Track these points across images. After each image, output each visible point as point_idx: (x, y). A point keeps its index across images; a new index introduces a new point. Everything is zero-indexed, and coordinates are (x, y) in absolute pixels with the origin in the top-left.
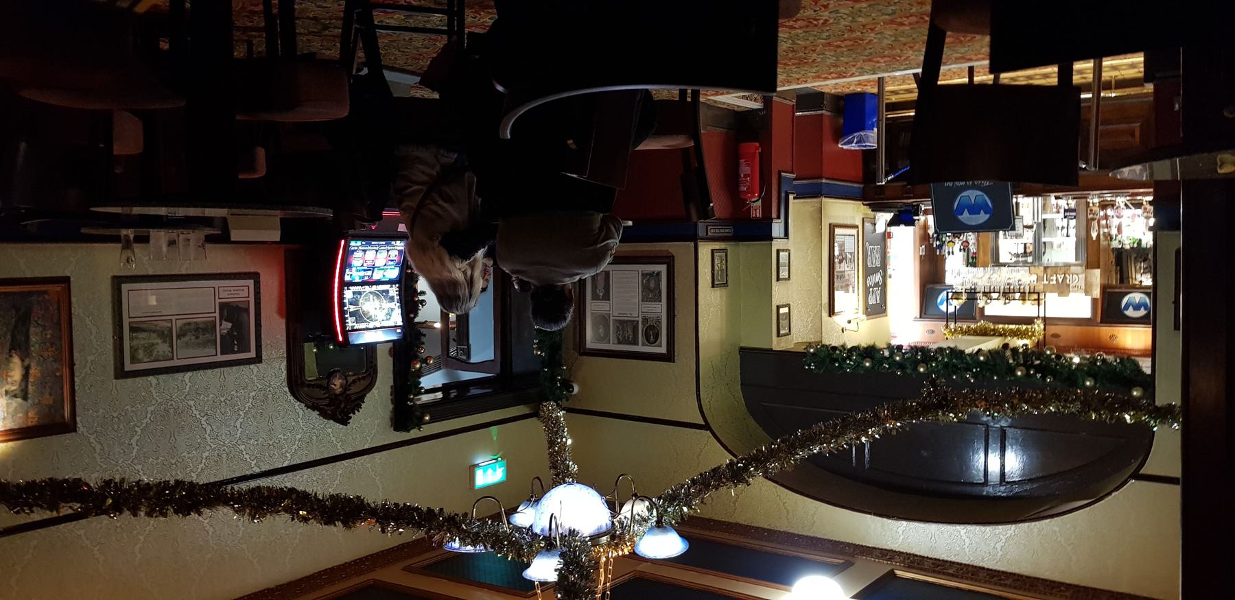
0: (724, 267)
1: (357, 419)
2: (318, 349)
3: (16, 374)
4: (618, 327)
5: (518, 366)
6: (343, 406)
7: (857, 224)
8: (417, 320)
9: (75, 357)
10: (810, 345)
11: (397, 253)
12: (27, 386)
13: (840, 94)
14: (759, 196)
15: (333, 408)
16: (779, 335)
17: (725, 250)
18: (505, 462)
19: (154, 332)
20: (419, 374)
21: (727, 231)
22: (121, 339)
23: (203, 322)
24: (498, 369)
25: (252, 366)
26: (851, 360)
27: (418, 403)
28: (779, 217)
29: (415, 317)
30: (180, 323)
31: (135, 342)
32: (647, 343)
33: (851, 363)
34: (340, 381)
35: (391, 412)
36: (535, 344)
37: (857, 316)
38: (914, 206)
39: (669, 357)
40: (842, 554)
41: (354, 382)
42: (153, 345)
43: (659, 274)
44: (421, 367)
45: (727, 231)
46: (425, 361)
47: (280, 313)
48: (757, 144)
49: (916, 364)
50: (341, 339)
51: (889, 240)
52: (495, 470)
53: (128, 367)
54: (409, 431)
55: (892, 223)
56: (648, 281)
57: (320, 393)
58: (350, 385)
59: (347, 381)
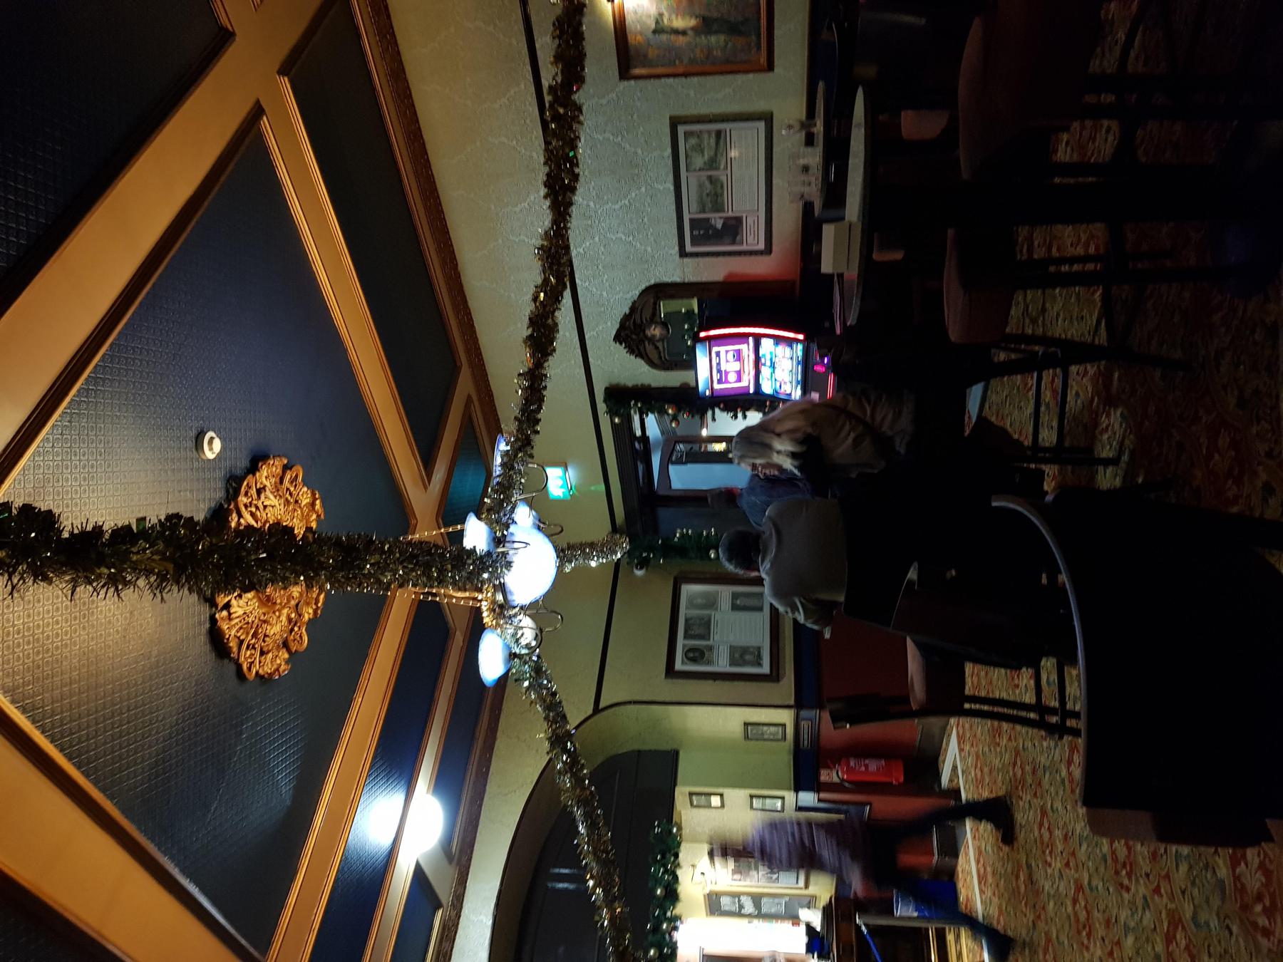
0: (766, 737)
1: (620, 350)
2: (685, 313)
3: (679, 23)
4: (703, 619)
5: (664, 513)
6: (634, 337)
7: (811, 888)
8: (717, 410)
9: (692, 78)
10: (680, 828)
11: (788, 392)
12: (667, 32)
13: (956, 877)
14: (843, 780)
15: (632, 327)
16: (691, 794)
17: (784, 738)
18: (569, 497)
19: (716, 155)
20: (662, 412)
21: (806, 742)
22: (710, 121)
23: (723, 200)
24: (661, 493)
25: (677, 248)
26: (663, 873)
27: (632, 412)
28: (819, 800)
29: (720, 408)
30: (724, 178)
31: (706, 136)
32: (685, 650)
33: (660, 874)
34: (658, 334)
35: (625, 385)
36: (687, 531)
37: (709, 882)
38: (829, 955)
39: (670, 672)
40: (461, 851)
41: (657, 348)
42: (702, 152)
43: (760, 665)
44: (668, 414)
45: (806, 742)
46: (675, 418)
47: (730, 275)
48: (902, 780)
49: (660, 948)
50: (703, 334)
51: (791, 922)
52: (562, 487)
53: (681, 129)
54: (605, 401)
55: (810, 929)
56: (752, 653)
57: (647, 314)
58: (654, 344)
59: (658, 341)
